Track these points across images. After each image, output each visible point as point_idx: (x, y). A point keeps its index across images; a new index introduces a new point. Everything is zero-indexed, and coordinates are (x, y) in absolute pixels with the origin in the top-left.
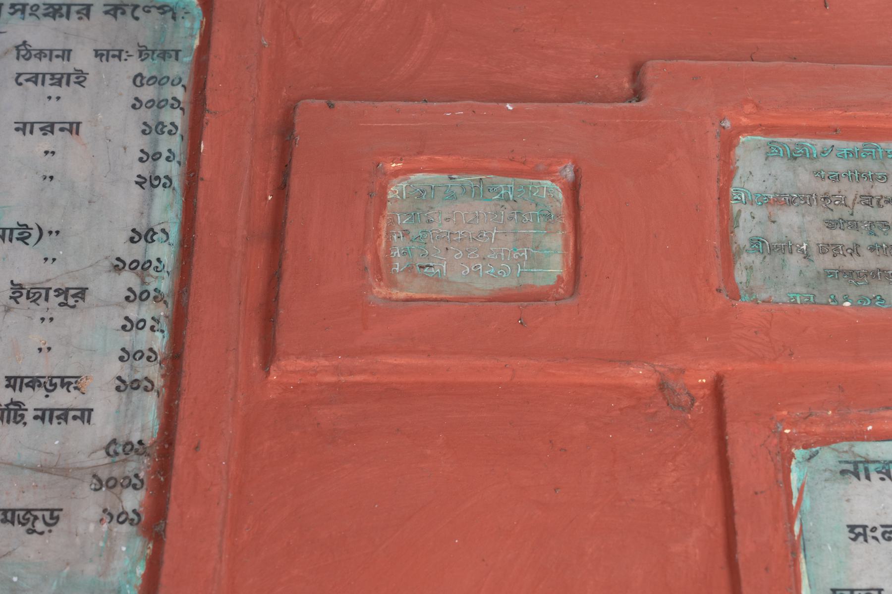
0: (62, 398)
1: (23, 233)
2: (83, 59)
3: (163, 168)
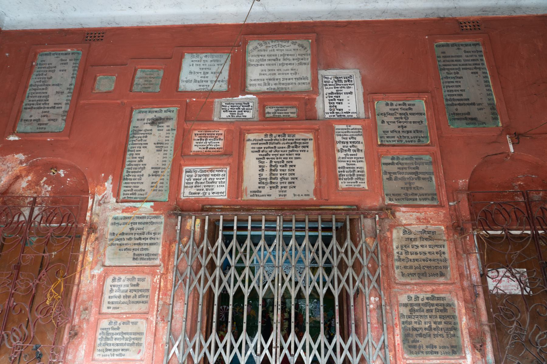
0: (60, 106)
1: (58, 85)
2: (68, 61)
3: (75, 76)
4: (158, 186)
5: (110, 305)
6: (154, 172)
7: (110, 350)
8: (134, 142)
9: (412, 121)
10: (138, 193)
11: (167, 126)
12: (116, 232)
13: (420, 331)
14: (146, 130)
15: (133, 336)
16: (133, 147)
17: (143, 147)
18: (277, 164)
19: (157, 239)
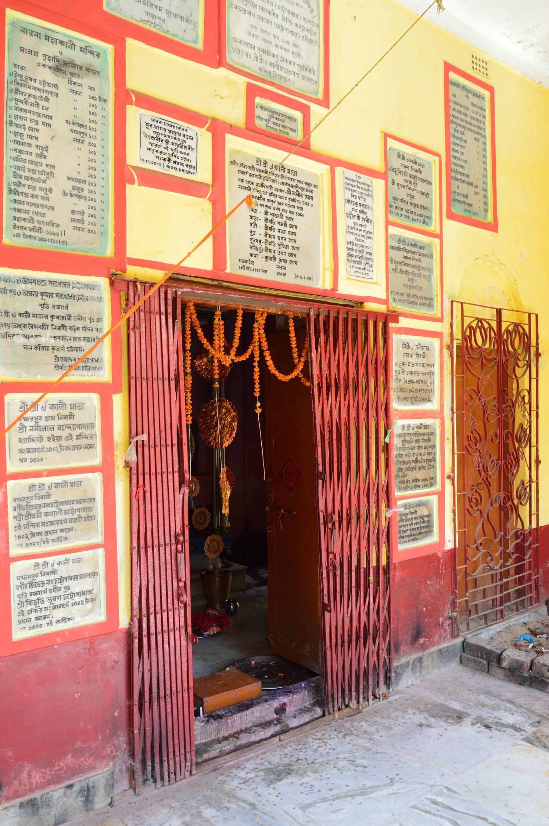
4: (86, 222)
5: (23, 456)
6: (74, 188)
7: (39, 534)
8: (21, 106)
9: (421, 190)
10: (45, 228)
11: (90, 88)
12: (11, 311)
13: (409, 465)
14: (44, 83)
15: (76, 506)
16: (21, 118)
17: (43, 123)
18: (274, 218)
19: (97, 330)
